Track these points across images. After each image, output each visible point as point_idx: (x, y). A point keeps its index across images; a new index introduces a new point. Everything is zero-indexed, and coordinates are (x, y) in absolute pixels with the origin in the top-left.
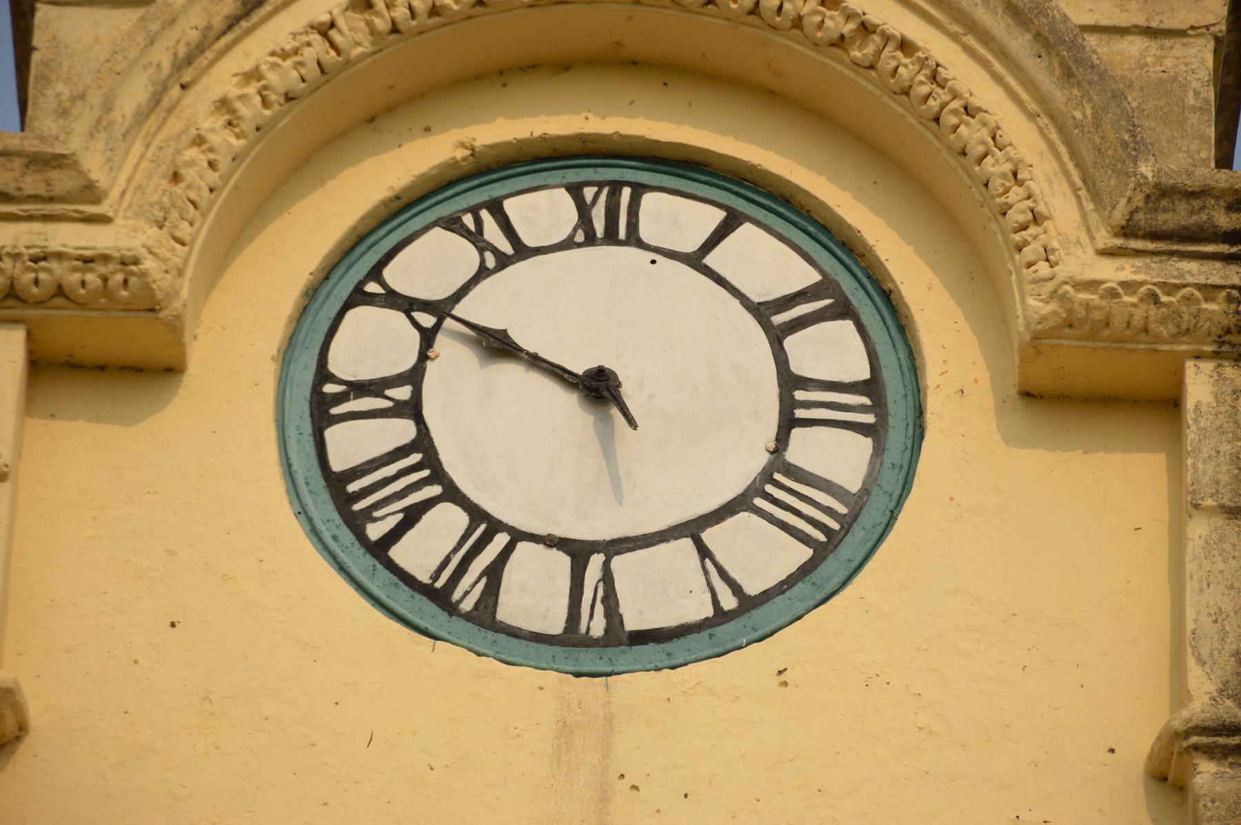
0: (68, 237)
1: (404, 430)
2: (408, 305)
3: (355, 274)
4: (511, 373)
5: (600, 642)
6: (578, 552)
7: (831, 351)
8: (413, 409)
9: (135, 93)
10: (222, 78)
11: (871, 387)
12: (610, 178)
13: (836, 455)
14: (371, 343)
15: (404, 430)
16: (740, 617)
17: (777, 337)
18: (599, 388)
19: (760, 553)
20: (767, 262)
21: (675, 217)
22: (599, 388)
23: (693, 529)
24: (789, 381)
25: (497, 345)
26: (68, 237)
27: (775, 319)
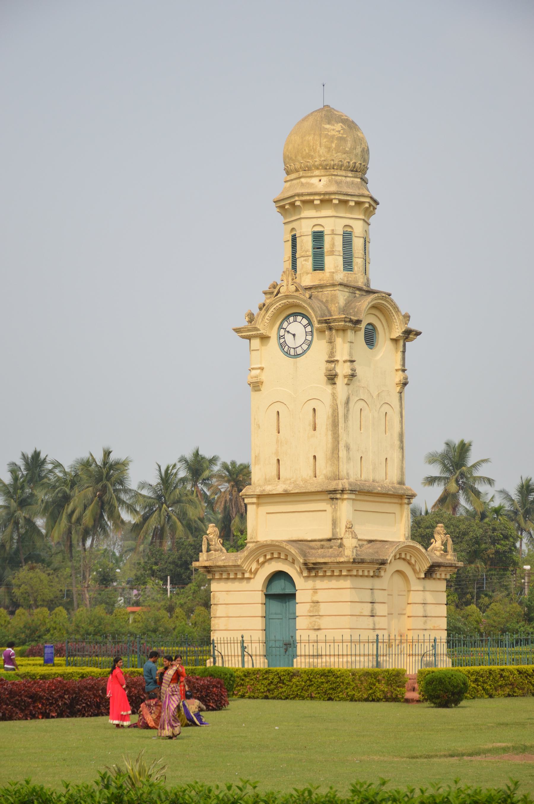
0: (259, 332)
1: (284, 340)
2: (284, 329)
3: (281, 327)
4: (289, 334)
5: (297, 356)
6: (294, 348)
7: (309, 329)
8: (284, 338)
9: (260, 320)
10: (267, 317)
11: (311, 331)
12: (295, 314)
13: (309, 338)
14: (282, 332)
15: (284, 340)
16: (304, 352)
17: (305, 328)
18: (294, 335)
19: (305, 347)
20: (305, 322)
21: (299, 318)
22: (294, 335)
23: (300, 346)
24: (306, 332)
25: (288, 332)
26: (259, 332)
27: (305, 327)
